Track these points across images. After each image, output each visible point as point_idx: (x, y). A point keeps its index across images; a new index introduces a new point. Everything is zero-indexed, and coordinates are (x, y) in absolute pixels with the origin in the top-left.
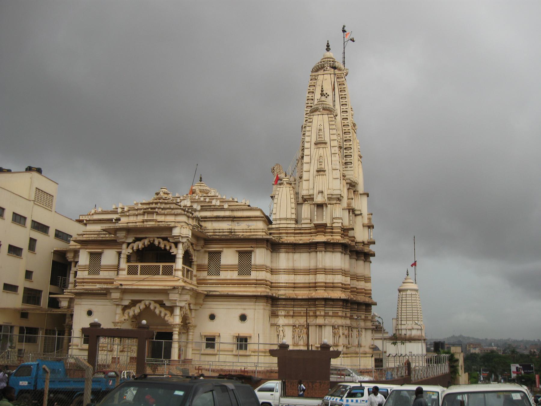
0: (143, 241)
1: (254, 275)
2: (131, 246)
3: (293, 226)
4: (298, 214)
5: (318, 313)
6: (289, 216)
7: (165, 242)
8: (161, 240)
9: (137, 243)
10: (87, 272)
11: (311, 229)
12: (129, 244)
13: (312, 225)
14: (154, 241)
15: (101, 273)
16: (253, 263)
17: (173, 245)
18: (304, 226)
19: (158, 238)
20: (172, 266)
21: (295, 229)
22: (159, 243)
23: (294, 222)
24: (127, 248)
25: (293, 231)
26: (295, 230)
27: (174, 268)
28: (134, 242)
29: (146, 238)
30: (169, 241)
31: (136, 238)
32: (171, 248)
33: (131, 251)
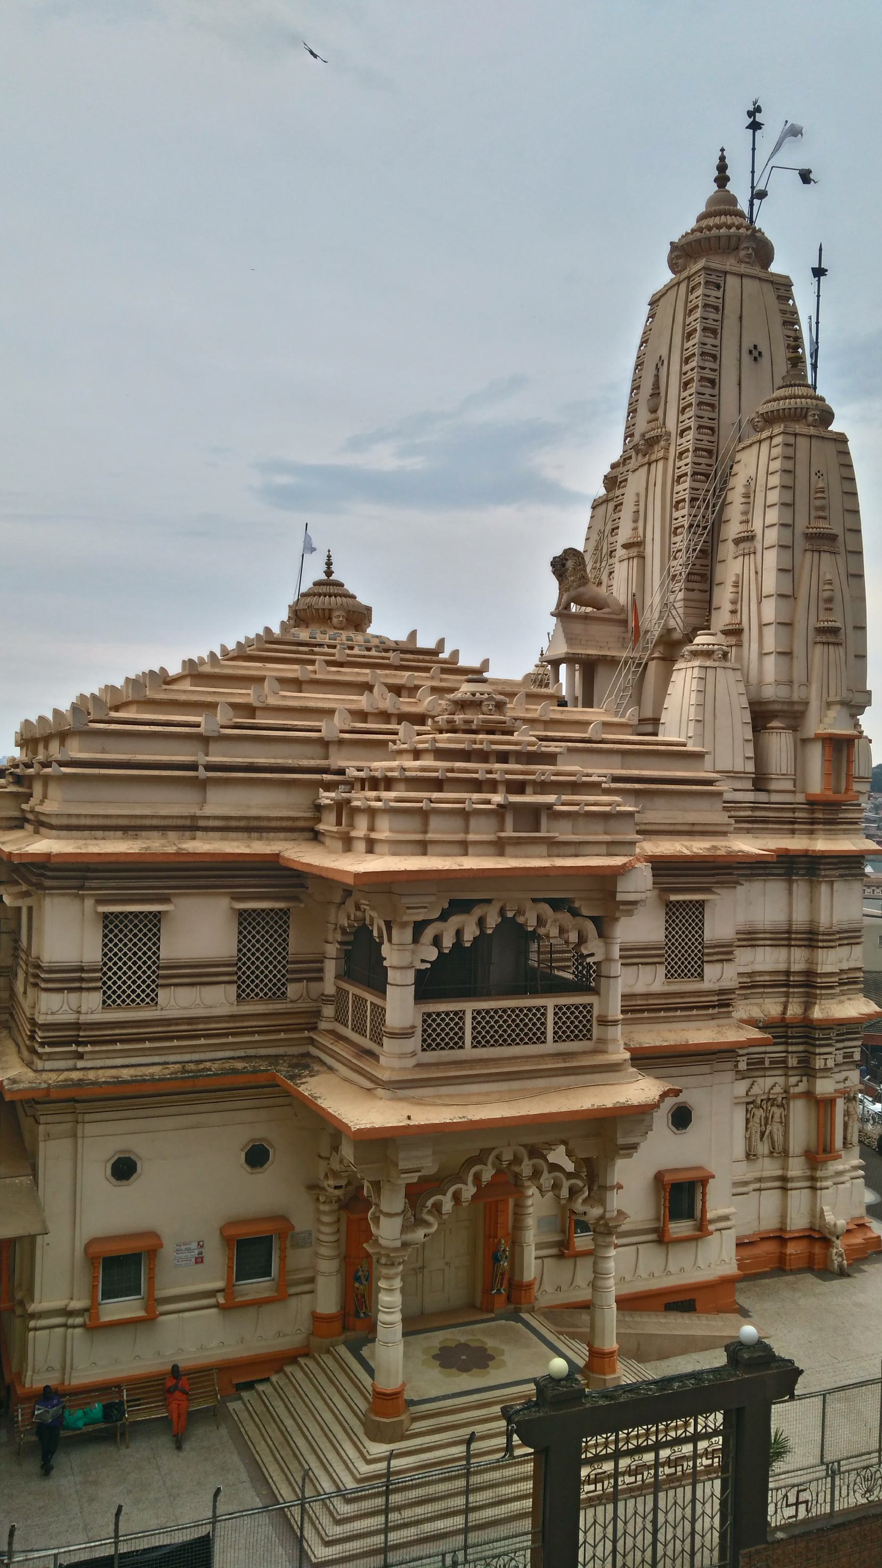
0: (478, 912)
1: (717, 976)
2: (429, 934)
3: (750, 796)
4: (760, 757)
5: (819, 1063)
6: (739, 767)
7: (565, 917)
8: (546, 909)
9: (455, 921)
10: (96, 998)
11: (793, 810)
12: (419, 928)
13: (800, 798)
14: (520, 912)
15: (163, 995)
16: (708, 935)
17: (590, 928)
18: (775, 798)
19: (534, 900)
20: (588, 1007)
21: (755, 806)
22: (541, 922)
23: (749, 785)
24: (416, 940)
25: (749, 813)
26: (753, 809)
27: (595, 1013)
28: (444, 917)
29: (489, 901)
30: (575, 913)
31: (452, 902)
32: (582, 939)
33: (432, 954)
